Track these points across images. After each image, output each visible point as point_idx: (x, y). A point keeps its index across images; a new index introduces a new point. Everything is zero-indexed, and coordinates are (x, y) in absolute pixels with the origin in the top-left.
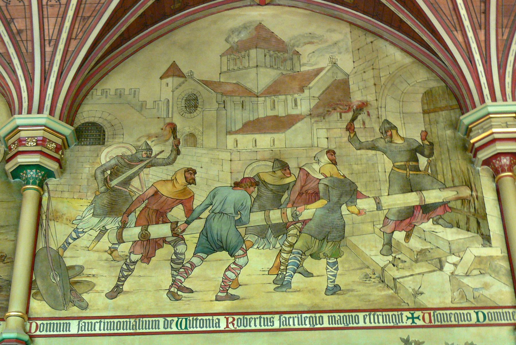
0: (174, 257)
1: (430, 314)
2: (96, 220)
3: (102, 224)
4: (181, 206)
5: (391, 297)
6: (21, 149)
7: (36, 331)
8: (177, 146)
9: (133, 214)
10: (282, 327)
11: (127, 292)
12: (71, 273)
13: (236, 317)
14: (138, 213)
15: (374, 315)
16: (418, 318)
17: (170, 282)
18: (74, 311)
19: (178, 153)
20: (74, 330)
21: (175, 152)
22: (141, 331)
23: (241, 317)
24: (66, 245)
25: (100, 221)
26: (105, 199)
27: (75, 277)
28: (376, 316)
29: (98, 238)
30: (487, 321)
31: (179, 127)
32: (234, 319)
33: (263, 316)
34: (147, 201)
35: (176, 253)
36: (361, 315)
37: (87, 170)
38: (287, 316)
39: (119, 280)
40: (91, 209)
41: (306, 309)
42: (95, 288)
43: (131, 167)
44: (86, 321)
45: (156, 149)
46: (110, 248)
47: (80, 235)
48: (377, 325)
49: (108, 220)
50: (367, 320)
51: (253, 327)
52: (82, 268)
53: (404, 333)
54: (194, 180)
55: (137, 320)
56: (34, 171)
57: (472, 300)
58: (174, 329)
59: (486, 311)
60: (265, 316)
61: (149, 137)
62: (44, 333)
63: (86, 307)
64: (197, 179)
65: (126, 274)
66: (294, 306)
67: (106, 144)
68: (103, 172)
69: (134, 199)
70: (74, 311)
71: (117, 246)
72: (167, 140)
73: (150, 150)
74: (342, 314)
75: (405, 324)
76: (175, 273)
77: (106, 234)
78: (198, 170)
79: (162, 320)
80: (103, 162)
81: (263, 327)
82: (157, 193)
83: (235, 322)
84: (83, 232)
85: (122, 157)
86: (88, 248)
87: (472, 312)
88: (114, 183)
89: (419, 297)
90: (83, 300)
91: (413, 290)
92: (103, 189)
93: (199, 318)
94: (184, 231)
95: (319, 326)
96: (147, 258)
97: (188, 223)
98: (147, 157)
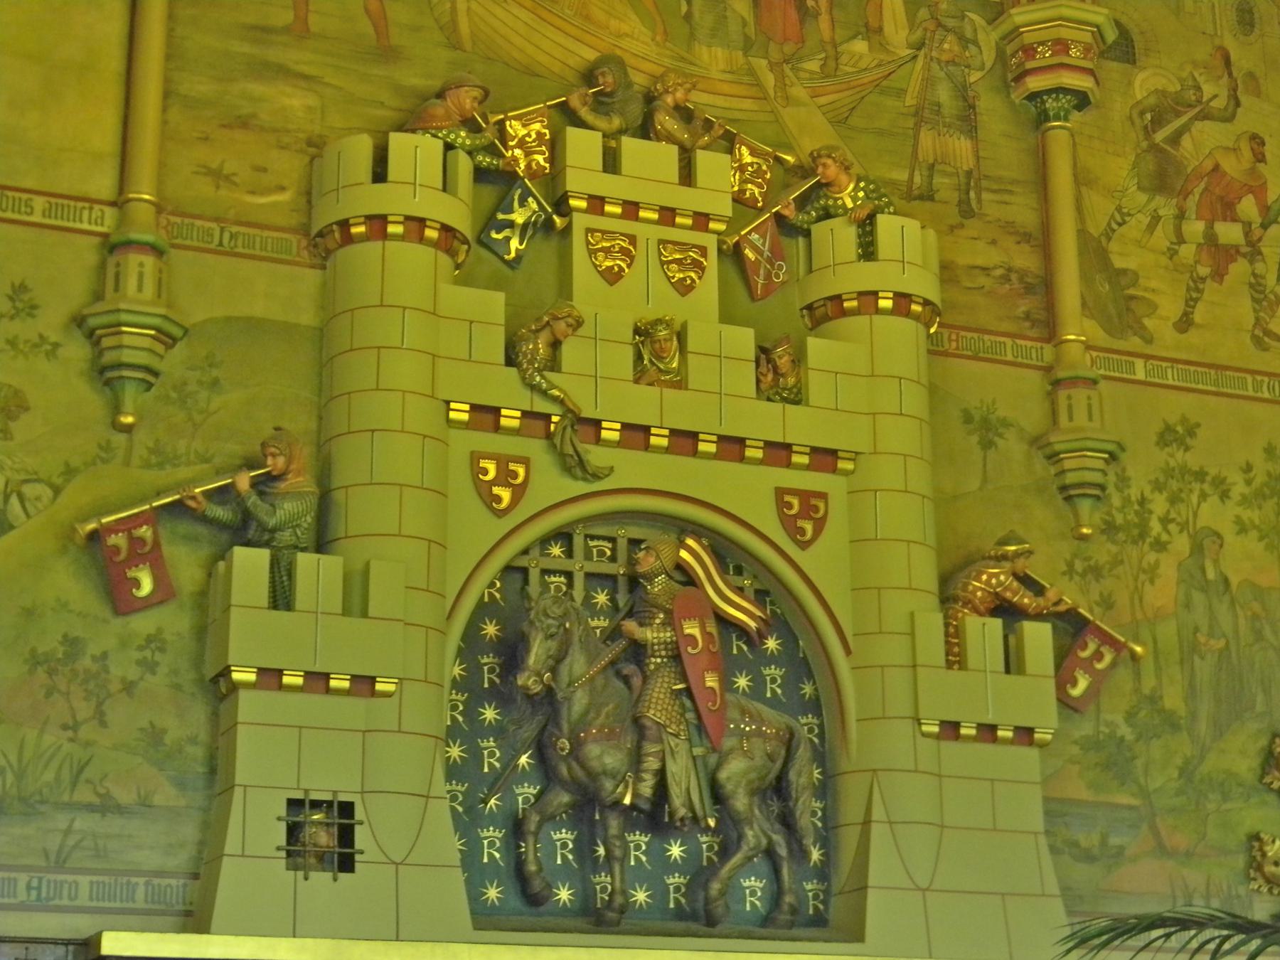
0: (1253, 280)
2: (1142, 198)
3: (1153, 205)
4: (1251, 197)
6: (1066, 60)
8: (1235, 90)
9: (1191, 196)
11: (1200, 326)
12: (1124, 281)
14: (1197, 197)
17: (1253, 321)
18: (1135, 343)
19: (1238, 104)
20: (1140, 375)
21: (1232, 103)
24: (1109, 233)
25: (1149, 201)
26: (1150, 164)
27: (1128, 288)
29: (1151, 228)
31: (1233, 57)
34: (1206, 179)
35: (1254, 275)
37: (1118, 108)
39: (1187, 305)
40: (1133, 177)
42: (1158, 311)
43: (1178, 114)
44: (1155, 362)
45: (1208, 90)
46: (1169, 249)
47: (1127, 219)
49: (1159, 200)
52: (1135, 274)
54: (1264, 156)
56: (1069, 97)
58: (1266, 395)
61: (1195, 64)
63: (1149, 340)
64: (1268, 156)
65: (1194, 295)
67: (1138, 64)
68: (1142, 113)
69: (1189, 170)
70: (1135, 343)
71: (1176, 247)
72: (1220, 77)
73: (1198, 88)
76: (1257, 307)
77: (1160, 224)
78: (1267, 139)
79: (1249, 378)
80: (1139, 97)
82: (1216, 168)
84: (1129, 215)
85: (1162, 93)
86: (1138, 243)
88: (1159, 136)
90: (1143, 327)
92: (1144, 144)
94: (1260, 239)
96: (1219, 275)
97: (1265, 226)
98: (1198, 101)
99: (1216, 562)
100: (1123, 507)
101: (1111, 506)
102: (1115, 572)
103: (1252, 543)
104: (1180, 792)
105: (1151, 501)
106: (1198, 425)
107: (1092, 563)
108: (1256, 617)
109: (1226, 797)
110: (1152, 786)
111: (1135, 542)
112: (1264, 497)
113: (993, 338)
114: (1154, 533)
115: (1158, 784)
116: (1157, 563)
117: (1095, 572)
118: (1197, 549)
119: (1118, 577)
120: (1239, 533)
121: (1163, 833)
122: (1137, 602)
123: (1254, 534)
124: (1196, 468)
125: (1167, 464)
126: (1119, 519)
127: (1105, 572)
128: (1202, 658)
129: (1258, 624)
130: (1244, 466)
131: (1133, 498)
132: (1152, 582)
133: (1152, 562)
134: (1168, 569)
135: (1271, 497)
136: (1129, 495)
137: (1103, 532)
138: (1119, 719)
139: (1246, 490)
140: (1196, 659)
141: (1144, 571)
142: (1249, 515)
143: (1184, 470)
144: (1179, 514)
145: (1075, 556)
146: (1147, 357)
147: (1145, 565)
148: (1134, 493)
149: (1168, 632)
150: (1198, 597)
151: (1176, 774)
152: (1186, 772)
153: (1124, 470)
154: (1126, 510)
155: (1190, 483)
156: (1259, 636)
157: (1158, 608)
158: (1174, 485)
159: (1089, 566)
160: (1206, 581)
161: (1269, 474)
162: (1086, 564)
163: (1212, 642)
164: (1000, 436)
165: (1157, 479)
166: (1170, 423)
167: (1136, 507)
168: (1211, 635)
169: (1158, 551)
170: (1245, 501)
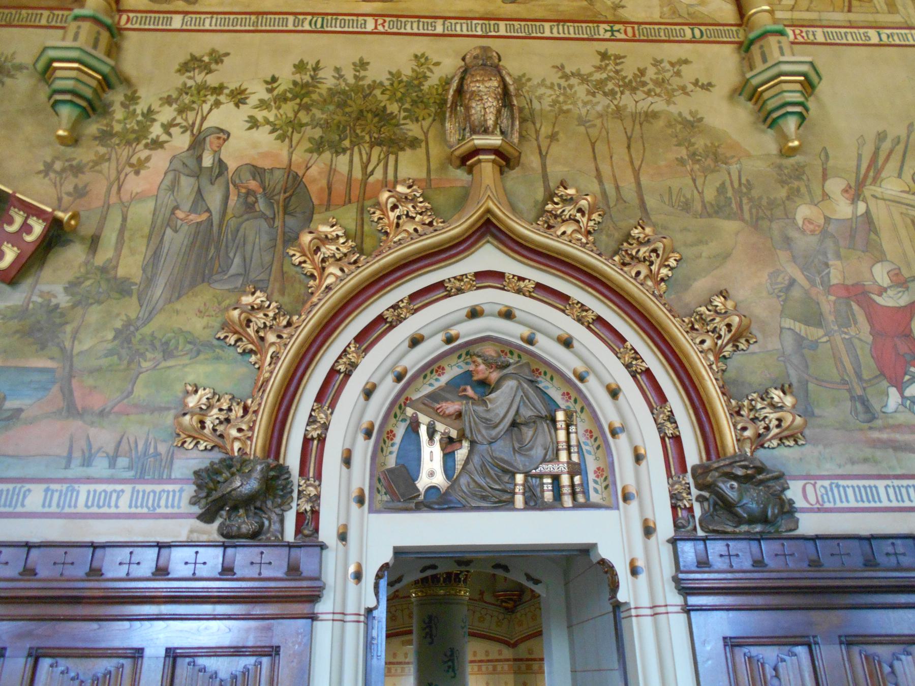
1: (633, 28)
5: (584, 8)
7: (127, 23)
10: (446, 32)
13: (387, 19)
15: (563, 26)
16: (618, 31)
22: (264, 28)
23: (395, 19)
28: (566, 27)
30: (705, 38)
32: (385, 21)
33: (422, 20)
36: (547, 25)
38: (453, 21)
41: (477, 15)
48: (567, 36)
50: (555, 30)
51: (409, 30)
53: (602, 47)
55: (260, 17)
57: (686, 16)
58: (307, 27)
59: (703, 28)
60: (425, 20)
62: (137, 26)
66: (462, 11)
74: (523, 23)
75: (601, 37)
81: (422, 31)
83: (386, 25)
87: (686, 28)
89: (621, 11)
91: (613, 3)
93: (340, 17)
95: (493, 34)
99: (216, 152)
100: (125, 119)
101: (112, 119)
102: (97, 168)
103: (264, 136)
104: (110, 353)
105: (158, 112)
106: (227, 54)
107: (74, 163)
108: (250, 192)
109: (168, 353)
110: (78, 348)
111: (129, 143)
112: (285, 100)
113: (30, 11)
114: (153, 136)
115: (86, 347)
116: (148, 159)
117: (77, 170)
118: (197, 144)
119: (100, 172)
120: (250, 128)
121: (77, 394)
122: (115, 188)
123: (268, 128)
124: (217, 85)
125: (185, 84)
126: (117, 128)
127: (86, 169)
128: (176, 231)
129: (251, 199)
130: (269, 79)
131: (139, 111)
132: (137, 173)
133: (143, 158)
134: (160, 161)
135: (291, 100)
136: (135, 110)
137: (95, 138)
138: (59, 289)
139: (266, 96)
140: (169, 231)
141: (132, 165)
142: (260, 115)
143: (202, 88)
144: (186, 120)
145: (56, 158)
146: (186, 13)
147: (134, 160)
148: (141, 107)
149: (142, 212)
150: (187, 184)
151: (110, 335)
152: (124, 335)
153: (135, 92)
154: (127, 121)
155: (205, 96)
156: (250, 207)
157: (137, 193)
158: (187, 99)
159: (71, 166)
160: (201, 168)
161: (295, 83)
162: (67, 164)
163: (192, 217)
164: (12, 76)
165: (169, 96)
166: (198, 55)
167: (140, 118)
168: (193, 209)
169: (151, 149)
170: (263, 105)
